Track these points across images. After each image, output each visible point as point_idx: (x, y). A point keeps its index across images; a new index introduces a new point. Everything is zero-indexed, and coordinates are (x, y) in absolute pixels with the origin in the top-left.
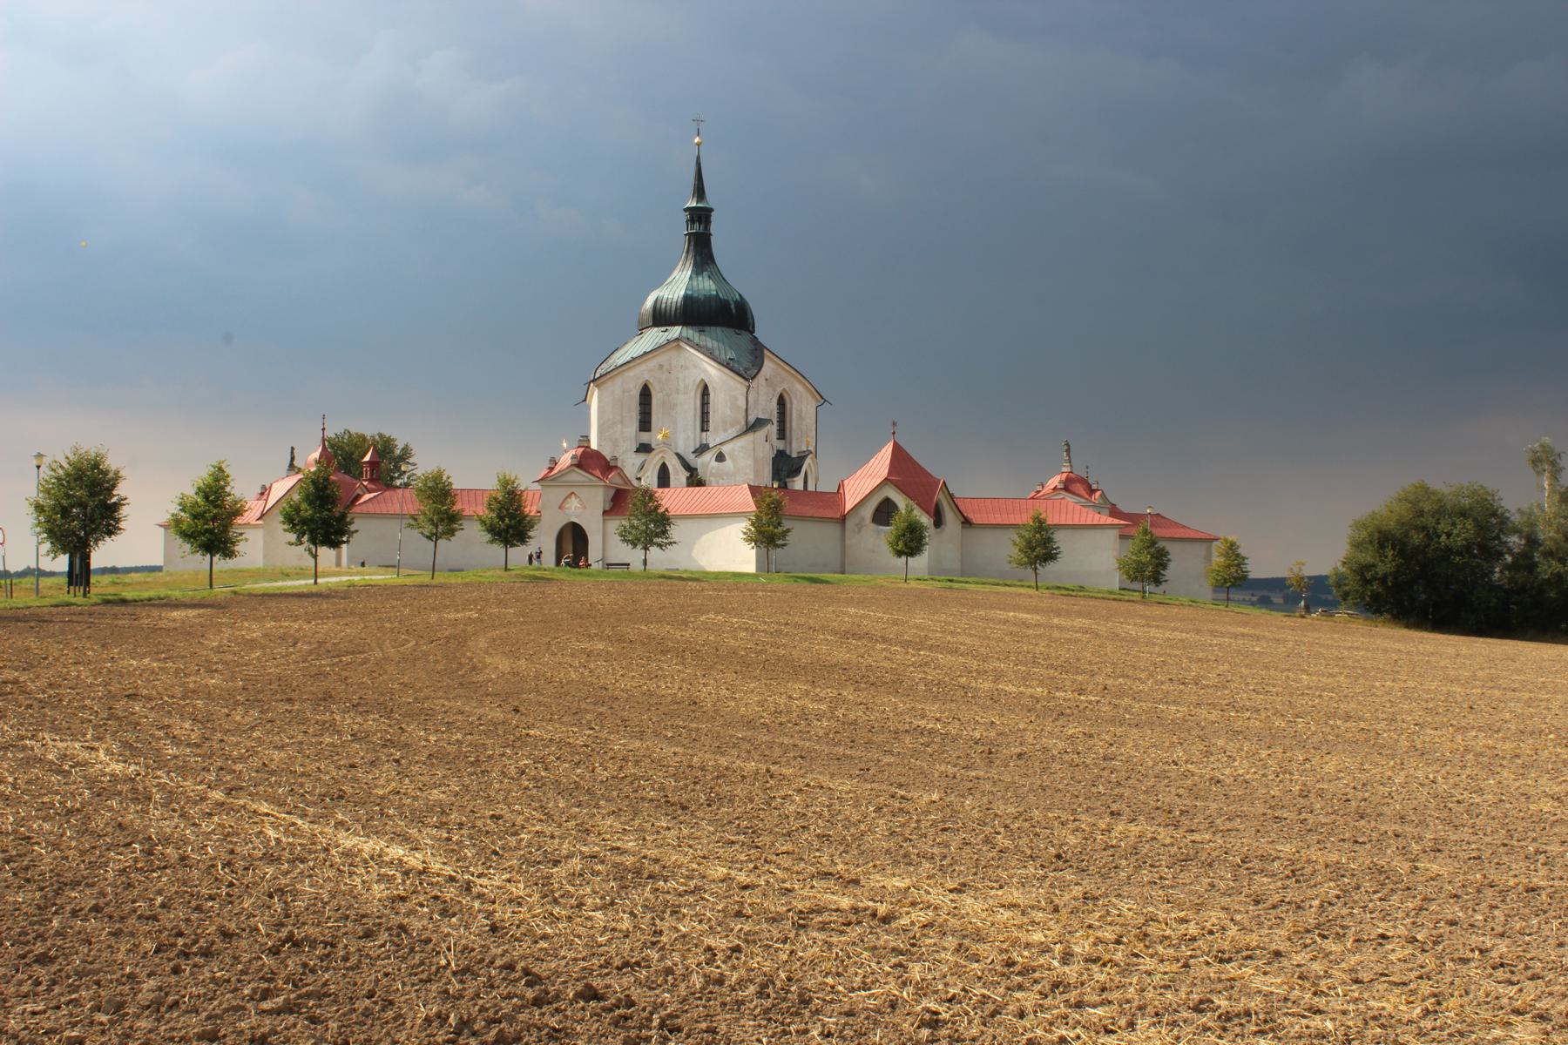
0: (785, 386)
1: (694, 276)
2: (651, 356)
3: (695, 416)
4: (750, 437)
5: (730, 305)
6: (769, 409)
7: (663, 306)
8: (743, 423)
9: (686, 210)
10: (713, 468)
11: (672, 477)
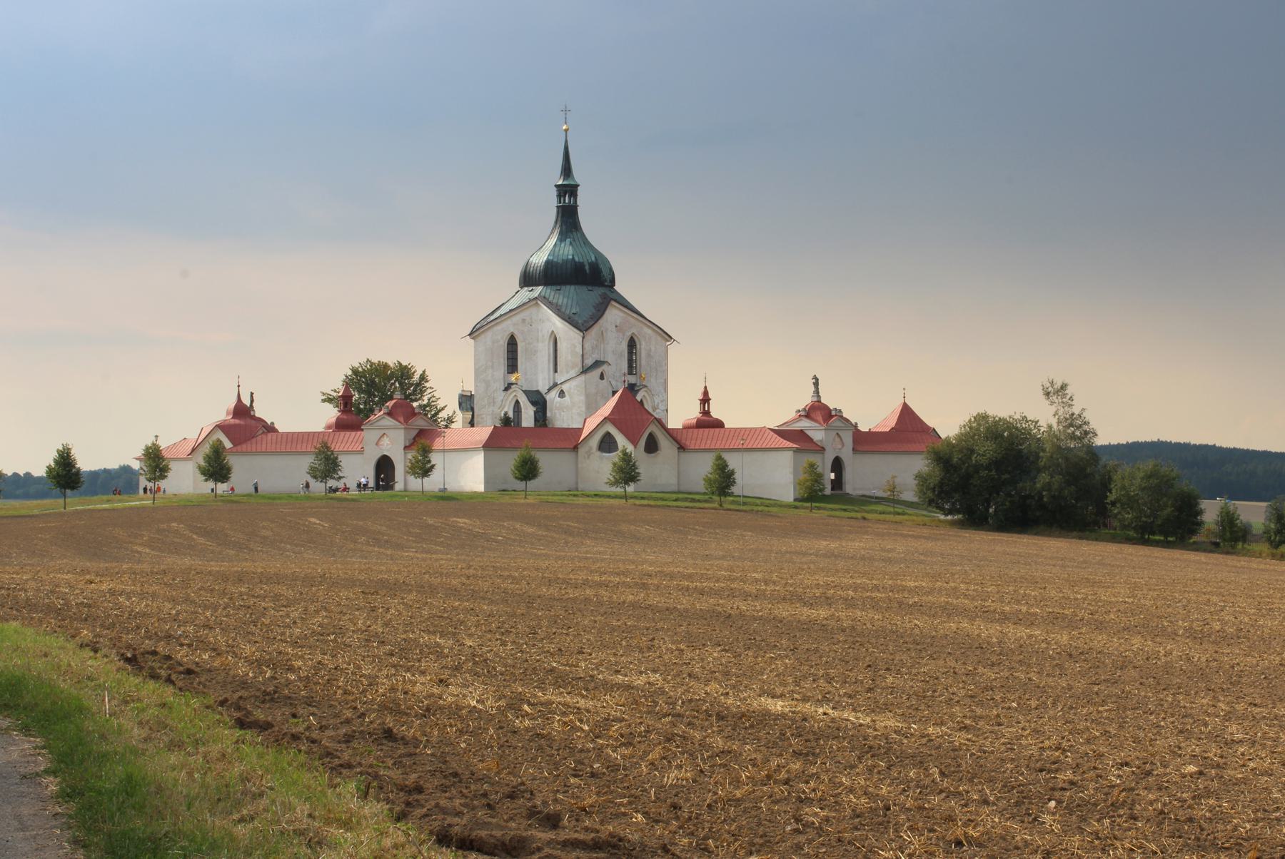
0: (634, 330)
1: (558, 243)
2: (514, 313)
3: (549, 360)
4: (583, 377)
5: (584, 266)
6: (614, 350)
7: (532, 269)
8: (580, 366)
9: (556, 186)
10: (557, 403)
11: (523, 411)
